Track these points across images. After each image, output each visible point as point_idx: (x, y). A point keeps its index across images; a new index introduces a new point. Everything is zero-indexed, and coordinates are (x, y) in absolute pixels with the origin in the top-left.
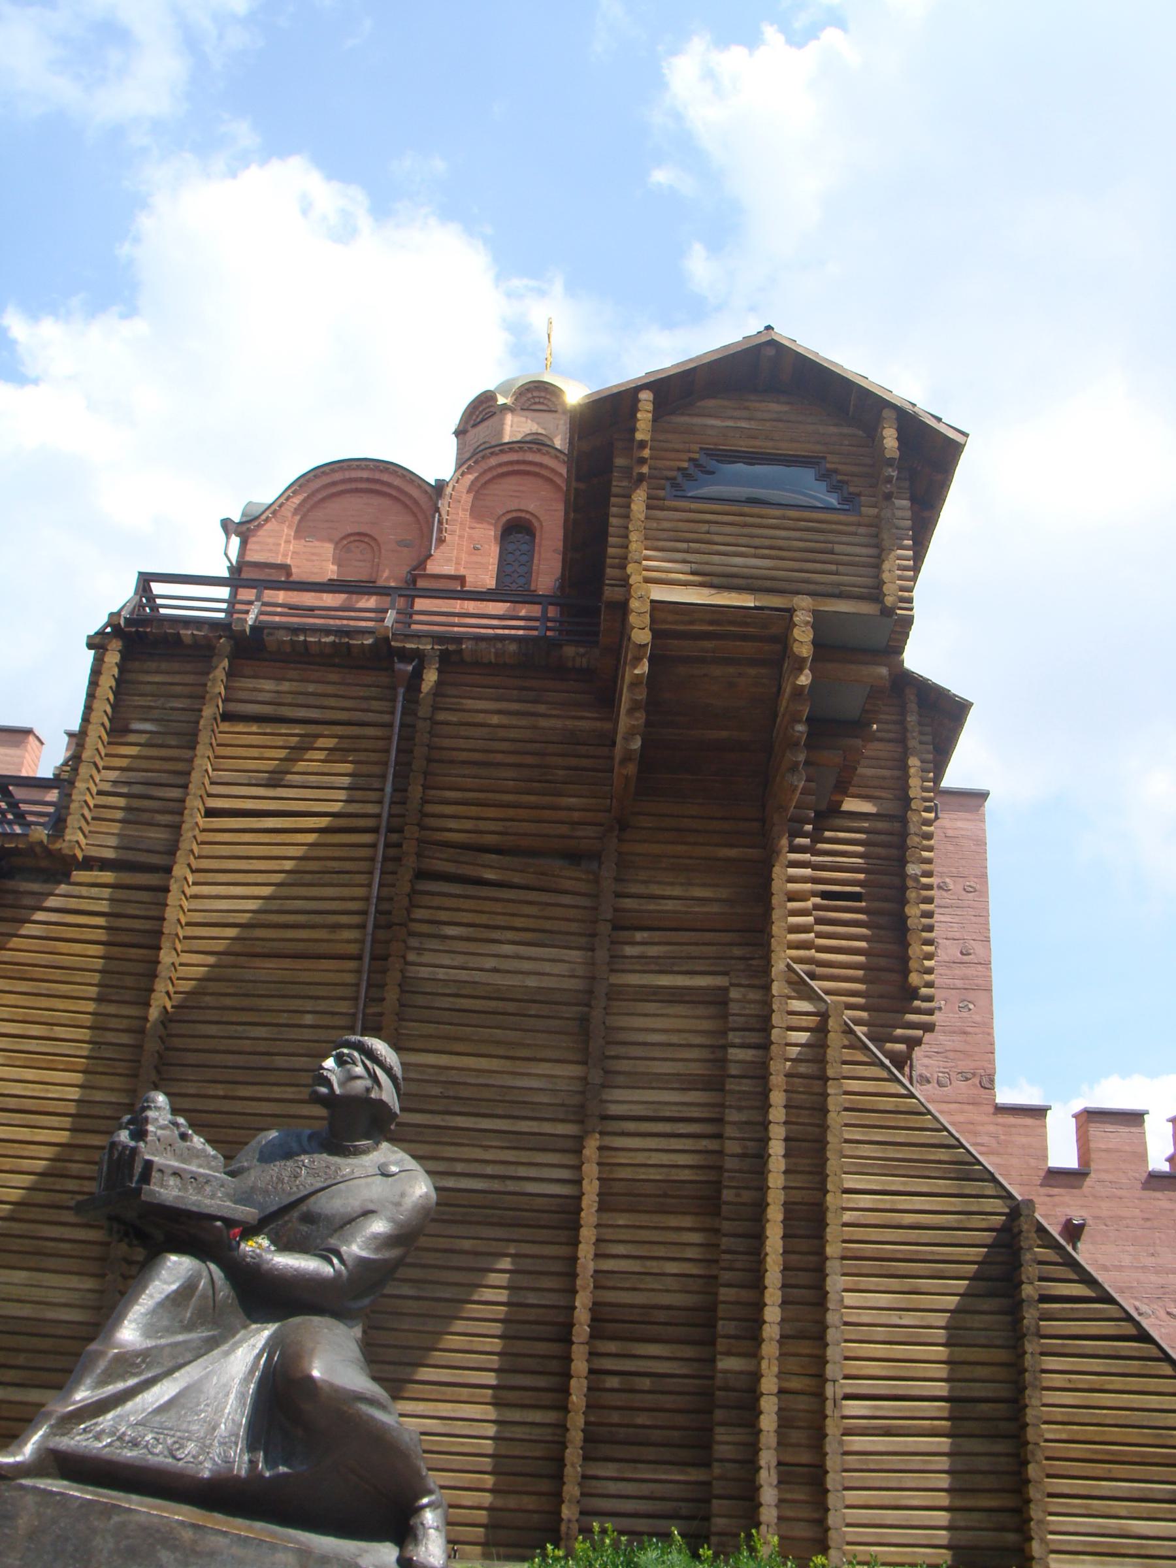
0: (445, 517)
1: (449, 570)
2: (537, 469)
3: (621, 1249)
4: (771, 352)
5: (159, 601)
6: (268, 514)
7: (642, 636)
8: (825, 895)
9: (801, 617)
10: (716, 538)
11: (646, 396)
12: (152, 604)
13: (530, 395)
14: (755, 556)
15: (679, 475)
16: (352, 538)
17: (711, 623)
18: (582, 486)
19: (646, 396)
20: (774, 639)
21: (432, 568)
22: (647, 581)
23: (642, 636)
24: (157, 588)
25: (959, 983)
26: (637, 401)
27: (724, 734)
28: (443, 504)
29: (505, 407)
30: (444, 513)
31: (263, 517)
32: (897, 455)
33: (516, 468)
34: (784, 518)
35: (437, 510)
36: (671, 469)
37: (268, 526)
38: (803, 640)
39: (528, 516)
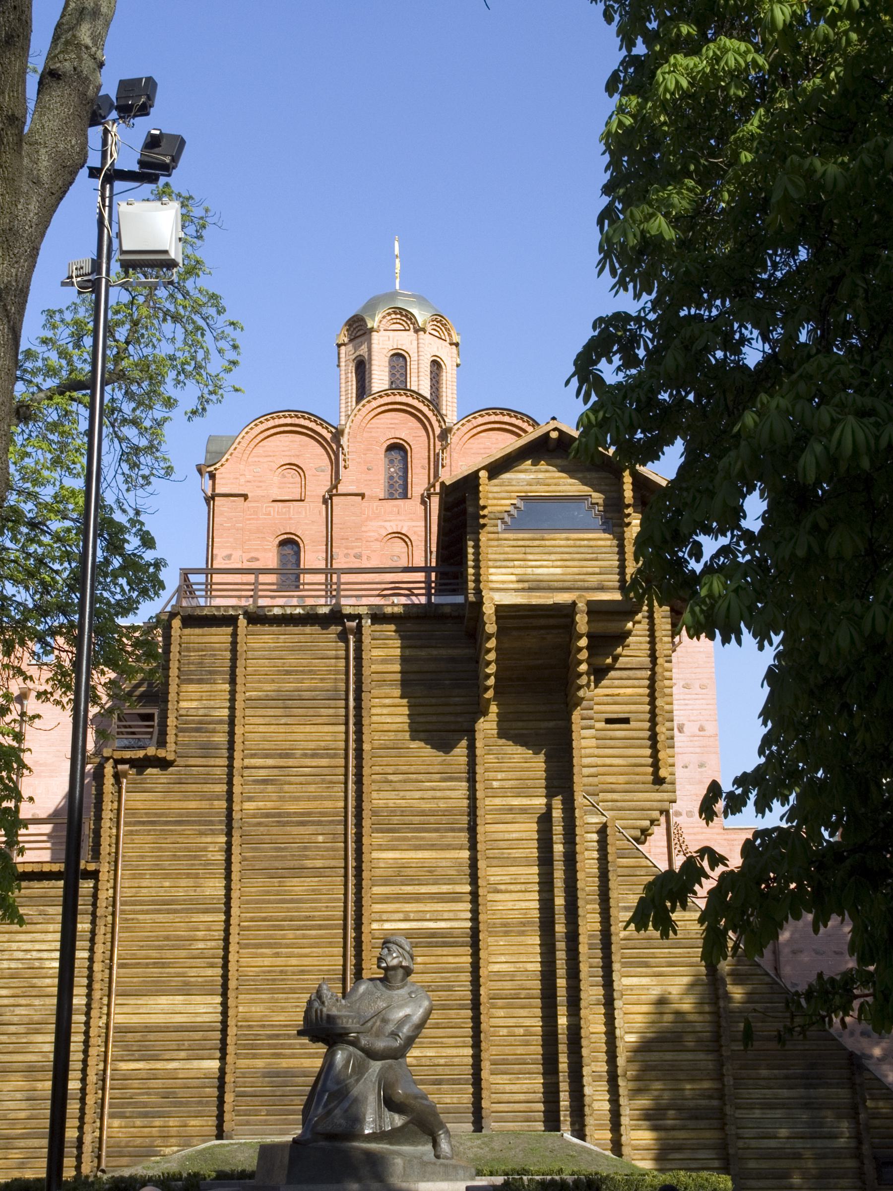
0: (346, 450)
1: (353, 489)
2: (405, 408)
3: (503, 959)
4: (554, 435)
5: (195, 587)
6: (226, 456)
7: (491, 628)
8: (609, 721)
9: (581, 606)
10: (530, 557)
11: (483, 474)
12: (190, 589)
13: (389, 318)
14: (553, 567)
15: (506, 515)
16: (285, 467)
17: (529, 610)
18: (449, 514)
19: (483, 474)
20: (566, 616)
21: (342, 489)
22: (492, 589)
23: (491, 628)
24: (193, 578)
25: (698, 750)
26: (478, 478)
27: (540, 662)
28: (344, 441)
29: (372, 330)
30: (345, 447)
31: (224, 459)
32: (631, 501)
33: (390, 407)
34: (568, 539)
35: (341, 446)
36: (501, 512)
37: (227, 465)
38: (582, 622)
39: (401, 442)
